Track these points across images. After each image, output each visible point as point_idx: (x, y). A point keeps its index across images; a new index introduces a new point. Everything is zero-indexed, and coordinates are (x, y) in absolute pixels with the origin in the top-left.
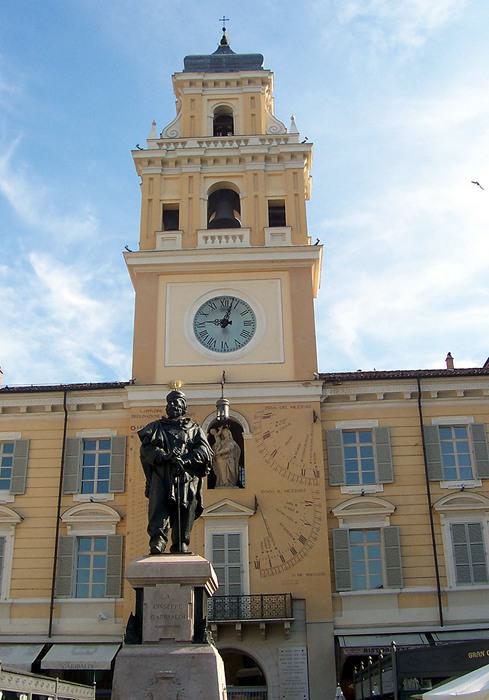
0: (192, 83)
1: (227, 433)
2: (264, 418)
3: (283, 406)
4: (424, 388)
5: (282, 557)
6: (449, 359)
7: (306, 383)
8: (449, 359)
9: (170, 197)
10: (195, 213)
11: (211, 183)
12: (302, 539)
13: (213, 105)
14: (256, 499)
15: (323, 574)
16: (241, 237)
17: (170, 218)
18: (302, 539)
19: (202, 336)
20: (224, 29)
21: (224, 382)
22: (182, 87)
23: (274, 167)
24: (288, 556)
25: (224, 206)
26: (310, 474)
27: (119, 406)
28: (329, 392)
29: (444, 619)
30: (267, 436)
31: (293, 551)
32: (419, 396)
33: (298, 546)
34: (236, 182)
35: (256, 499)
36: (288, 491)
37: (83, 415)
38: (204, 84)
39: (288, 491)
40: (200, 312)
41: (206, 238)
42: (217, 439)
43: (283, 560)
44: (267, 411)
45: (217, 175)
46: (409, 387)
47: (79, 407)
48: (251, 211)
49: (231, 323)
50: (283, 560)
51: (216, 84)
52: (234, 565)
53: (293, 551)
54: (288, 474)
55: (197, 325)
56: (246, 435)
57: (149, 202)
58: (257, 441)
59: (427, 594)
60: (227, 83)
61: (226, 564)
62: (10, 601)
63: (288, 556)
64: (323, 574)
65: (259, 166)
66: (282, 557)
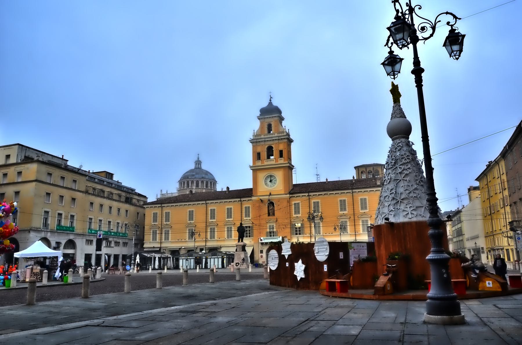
4: (310, 194)
6: (327, 180)
7: (286, 194)
8: (327, 180)
10: (264, 154)
11: (267, 146)
17: (259, 154)
19: (266, 184)
21: (270, 194)
23: (280, 141)
25: (270, 151)
32: (309, 196)
34: (273, 146)
40: (266, 179)
44: (279, 200)
46: (307, 194)
48: (276, 152)
55: (265, 182)
57: (254, 152)
65: (277, 142)
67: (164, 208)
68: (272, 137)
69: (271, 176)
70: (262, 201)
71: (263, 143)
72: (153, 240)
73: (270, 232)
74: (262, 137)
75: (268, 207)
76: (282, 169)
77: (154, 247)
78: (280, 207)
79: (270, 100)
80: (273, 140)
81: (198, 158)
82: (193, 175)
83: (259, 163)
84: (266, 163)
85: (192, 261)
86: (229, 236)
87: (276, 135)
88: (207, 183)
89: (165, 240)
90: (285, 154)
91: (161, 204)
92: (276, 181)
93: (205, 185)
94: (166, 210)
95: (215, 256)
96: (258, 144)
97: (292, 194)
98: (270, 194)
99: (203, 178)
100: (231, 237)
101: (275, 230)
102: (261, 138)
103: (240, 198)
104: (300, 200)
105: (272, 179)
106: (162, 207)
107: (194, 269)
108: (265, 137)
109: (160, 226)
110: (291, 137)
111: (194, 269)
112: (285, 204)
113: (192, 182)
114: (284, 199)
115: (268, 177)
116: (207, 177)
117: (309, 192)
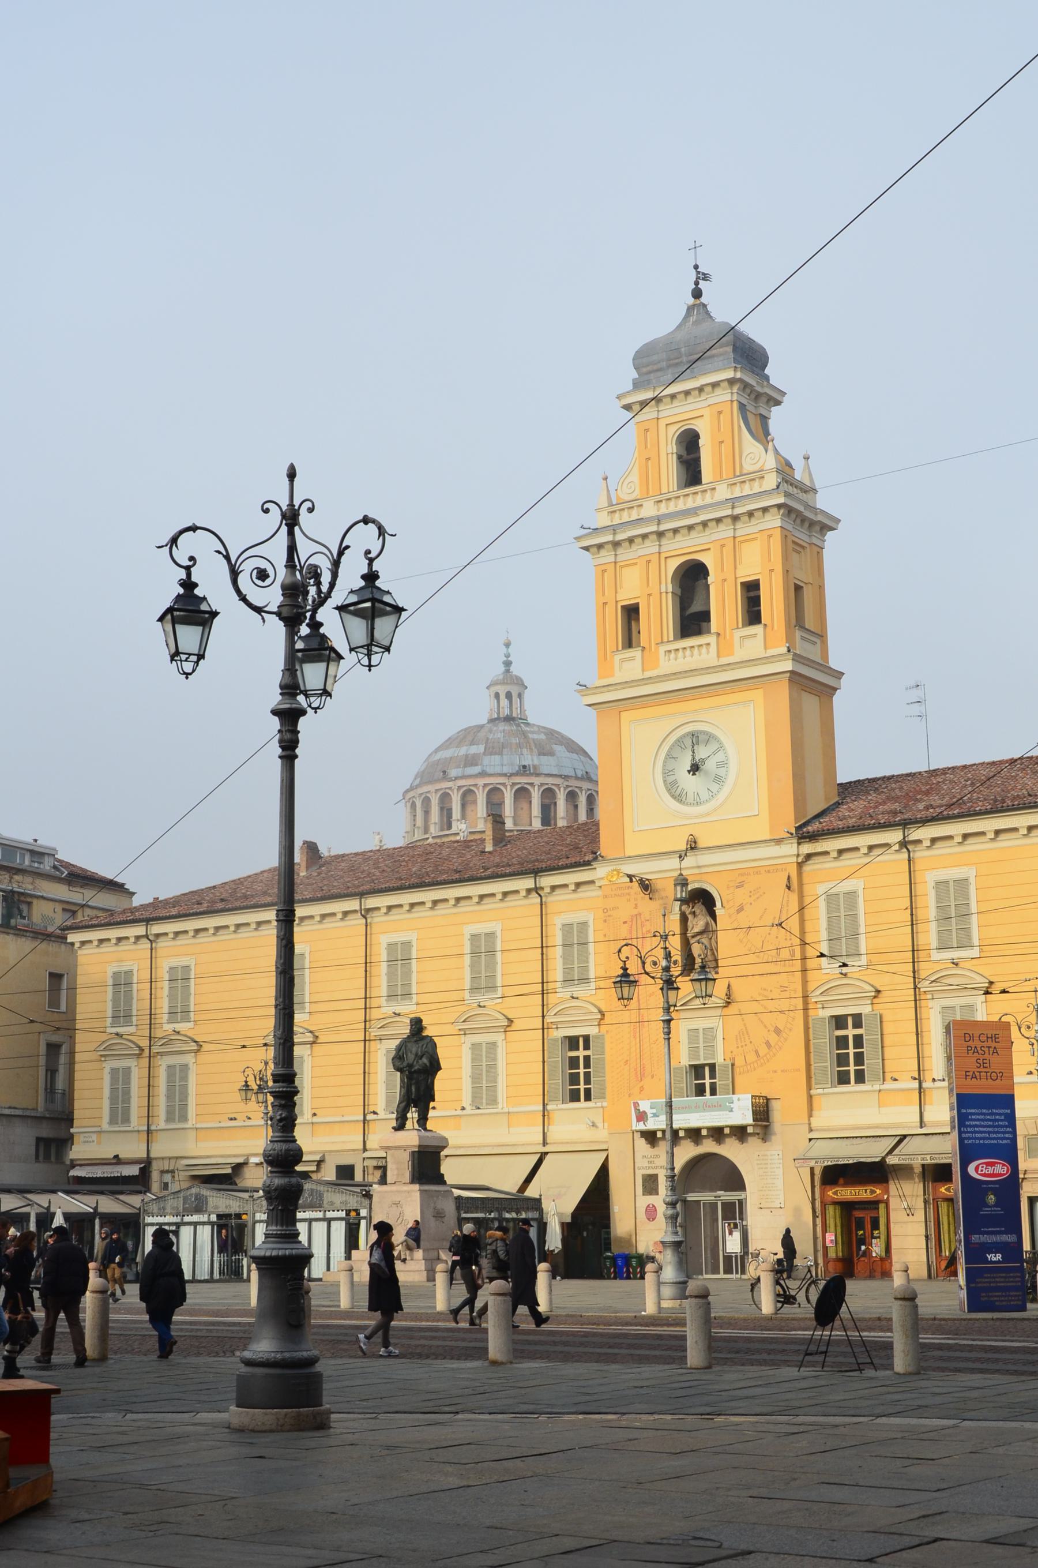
1: (699, 908)
2: (738, 887)
3: (757, 871)
5: (756, 1052)
7: (779, 841)
9: (627, 597)
11: (674, 564)
12: (778, 1031)
13: (674, 431)
15: (798, 1070)
18: (778, 1031)
20: (696, 267)
24: (763, 1050)
27: (592, 882)
29: (926, 1119)
30: (740, 909)
31: (768, 1044)
32: (904, 844)
33: (773, 1038)
34: (707, 559)
37: (560, 896)
40: (669, 756)
42: (690, 917)
43: (758, 1055)
44: (741, 878)
45: (680, 550)
46: (894, 836)
47: (553, 888)
48: (723, 601)
49: (689, 772)
50: (758, 1055)
53: (768, 1044)
55: (666, 773)
56: (719, 910)
58: (730, 916)
59: (913, 1089)
62: (506, 1110)
63: (763, 1050)
64: (798, 1070)
65: (725, 531)
66: (756, 1052)
67: (162, 943)
68: (694, 511)
69: (695, 738)
70: (646, 886)
71: (650, 547)
72: (113, 1121)
73: (697, 1070)
74: (649, 510)
75: (684, 919)
76: (757, 695)
77: (117, 1160)
78: (743, 920)
79: (697, 294)
80: (705, 524)
81: (508, 664)
82: (471, 761)
83: (629, 666)
84: (666, 665)
85: (205, 1233)
87: (723, 492)
88: (549, 794)
89: (170, 1118)
90: (773, 602)
91: (148, 921)
92: (722, 764)
93: (536, 810)
94: (173, 954)
95: (198, 1210)
96: (625, 554)
97: (813, 837)
98: (693, 846)
99: (524, 770)
100: (493, 1101)
101: (719, 1059)
102: (640, 520)
103: (536, 872)
104: (865, 873)
105: (702, 752)
106: (153, 940)
107: (211, 1280)
108: (663, 509)
109: (144, 1043)
110: (824, 502)
111: (211, 1280)
112: (776, 900)
113: (467, 795)
114: (769, 870)
115: (679, 742)
116: (547, 764)
117: (905, 824)
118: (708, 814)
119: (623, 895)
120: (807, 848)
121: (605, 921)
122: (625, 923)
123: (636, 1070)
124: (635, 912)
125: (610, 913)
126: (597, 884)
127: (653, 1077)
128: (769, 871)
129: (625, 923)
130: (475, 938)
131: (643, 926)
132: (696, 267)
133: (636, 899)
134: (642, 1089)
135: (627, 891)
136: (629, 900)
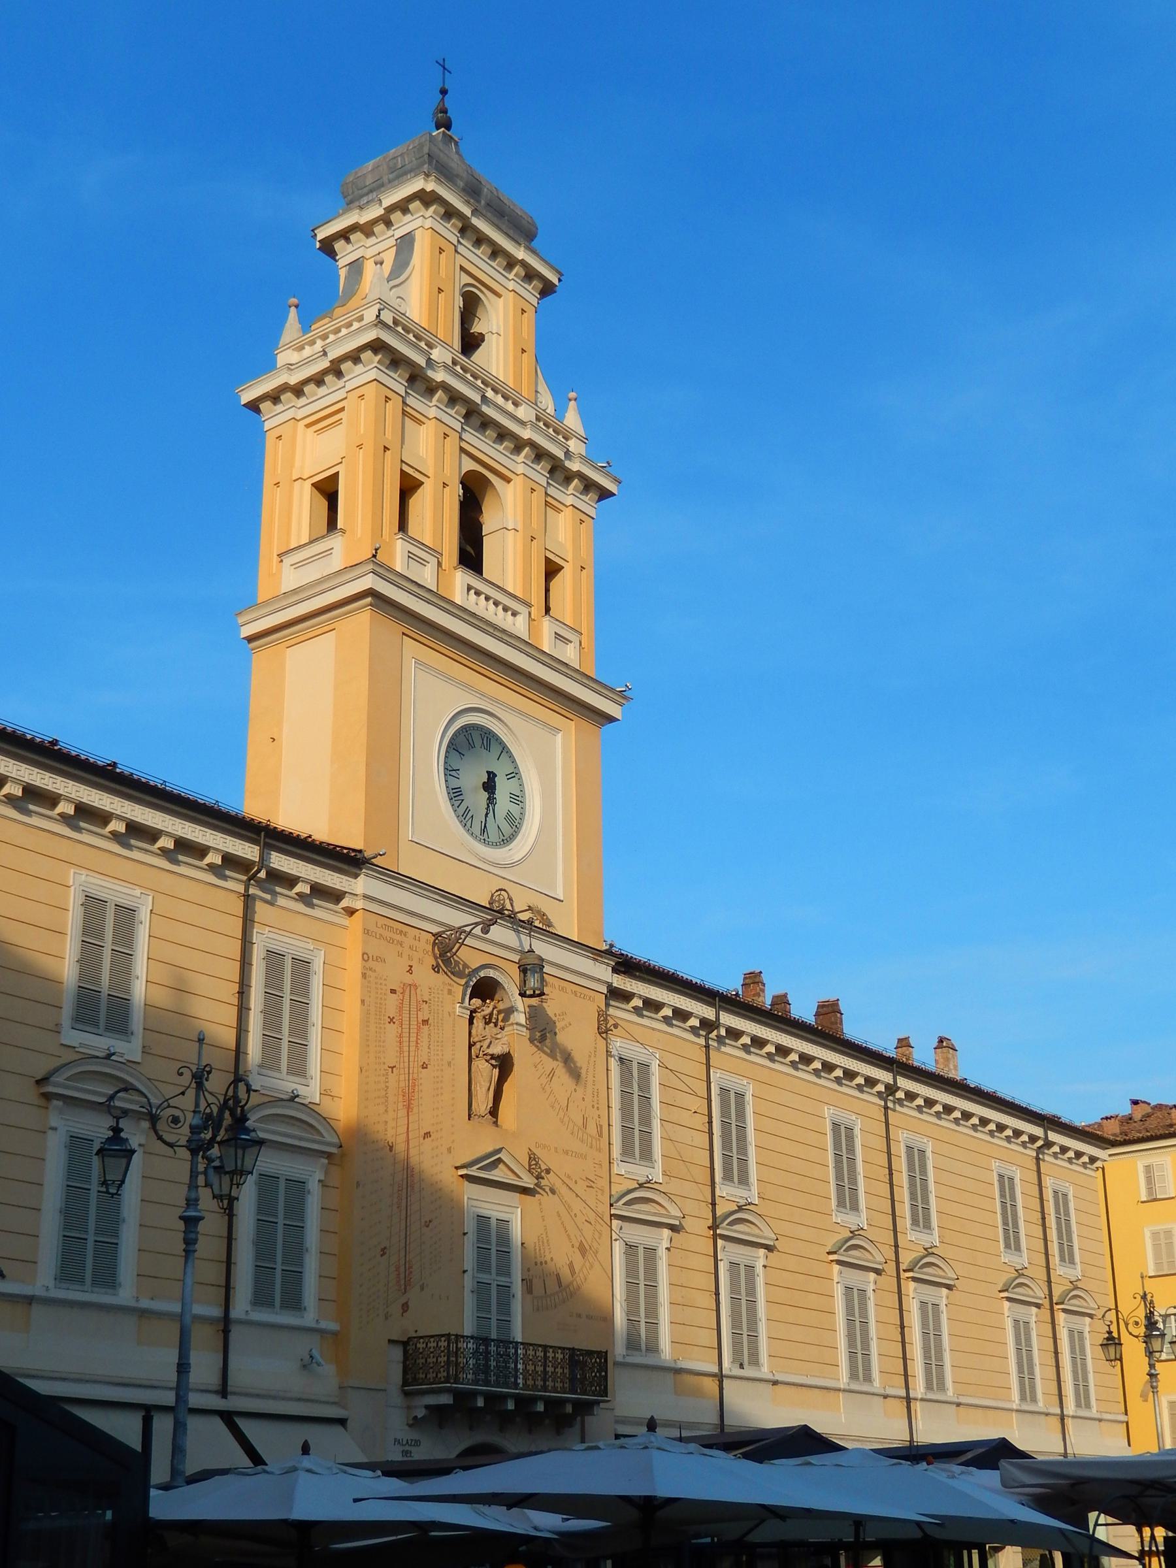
0: (450, 213)
7: (597, 954)
11: (469, 465)
12: (583, 1250)
14: (532, 1157)
16: (514, 614)
20: (444, 92)
22: (427, 204)
26: (592, 1129)
28: (620, 982)
35: (532, 1157)
36: (566, 1153)
38: (466, 229)
39: (566, 1153)
40: (451, 745)
41: (469, 588)
51: (480, 240)
52: (503, 1280)
54: (566, 1119)
60: (496, 252)
61: (492, 1278)
86: (88, 1254)
100: (107, 1277)
118: (504, 867)
119: (391, 941)
120: (620, 982)
121: (364, 975)
122: (393, 991)
123: (398, 1269)
124: (408, 979)
125: (371, 964)
126: (345, 903)
127: (422, 1288)
128: (575, 993)
129: (393, 991)
130: (93, 905)
131: (419, 1010)
132: (444, 92)
133: (410, 958)
134: (405, 1307)
135: (398, 937)
136: (400, 955)
